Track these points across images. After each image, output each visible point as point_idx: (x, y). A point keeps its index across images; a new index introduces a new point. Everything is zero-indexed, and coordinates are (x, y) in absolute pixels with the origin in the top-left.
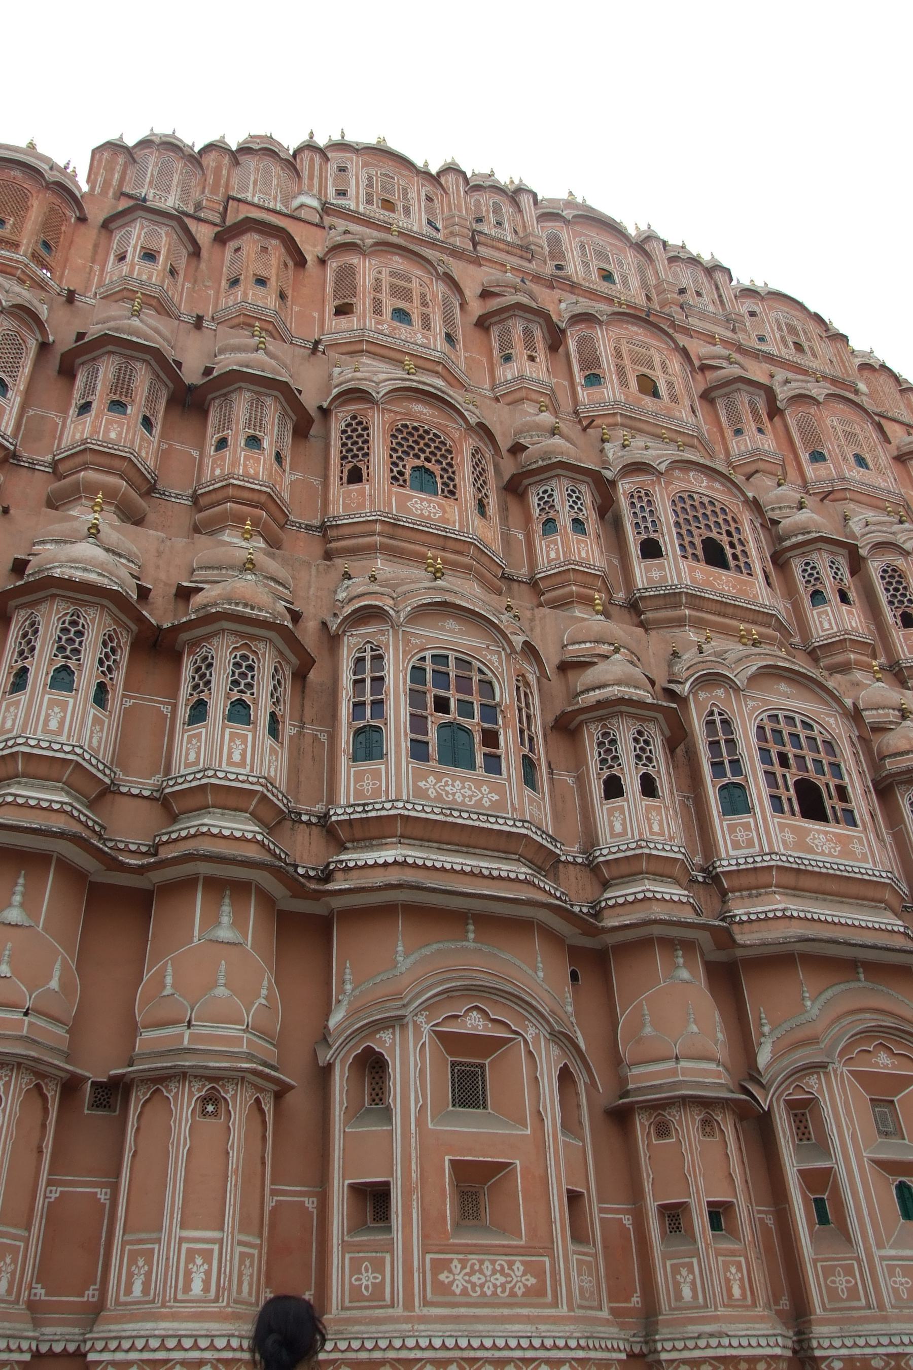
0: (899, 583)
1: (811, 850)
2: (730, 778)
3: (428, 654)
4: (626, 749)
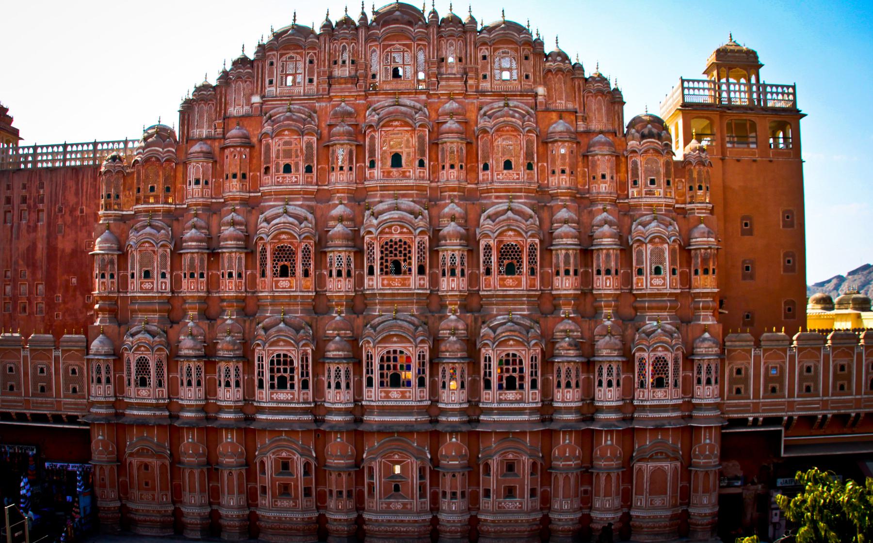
2: (370, 375)
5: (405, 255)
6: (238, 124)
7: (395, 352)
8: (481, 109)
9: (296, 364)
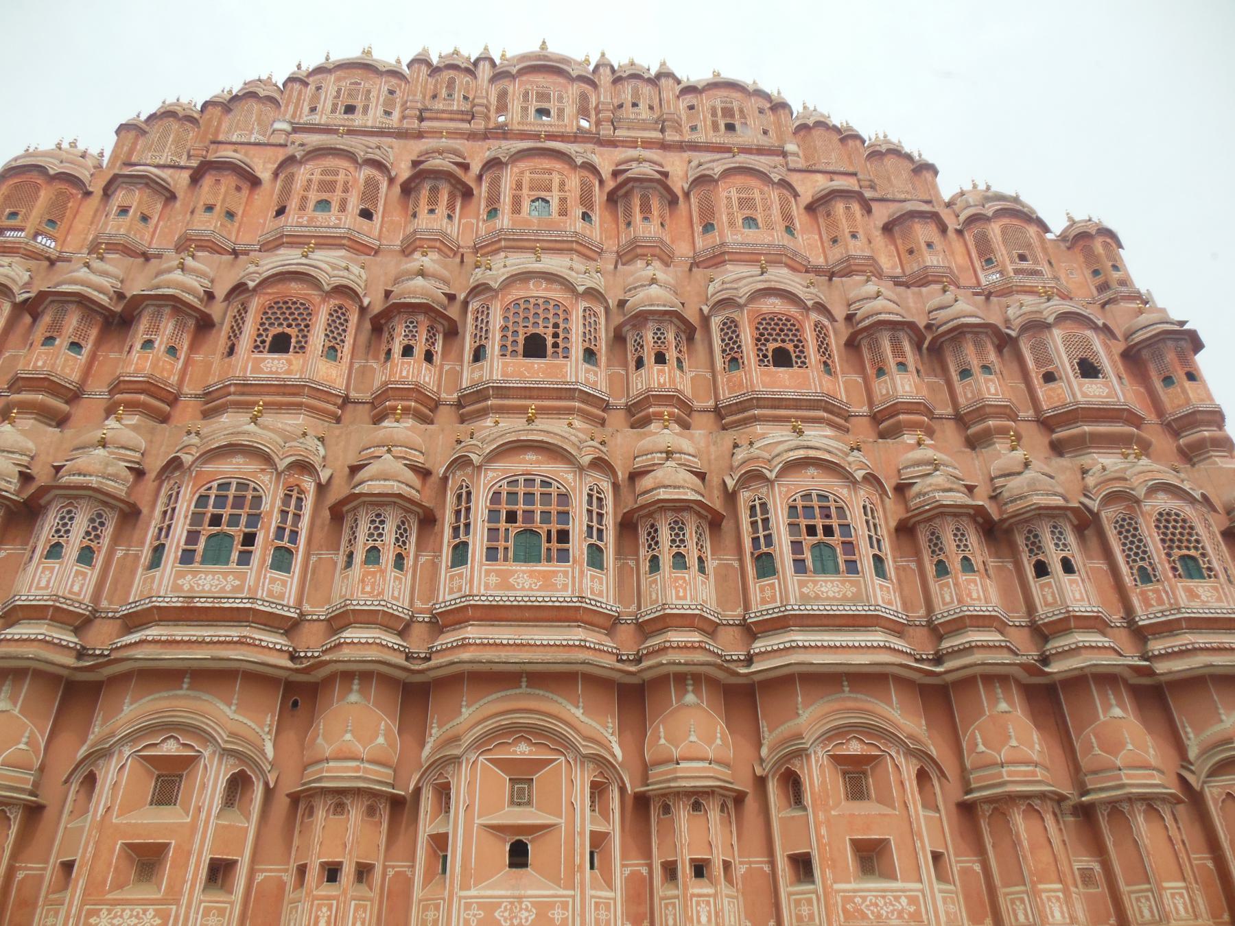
0: (734, 332)
1: (512, 588)
2: (463, 538)
3: (215, 484)
4: (390, 528)
5: (556, 326)
6: (235, 151)
7: (530, 482)
8: (690, 162)
9: (265, 506)
